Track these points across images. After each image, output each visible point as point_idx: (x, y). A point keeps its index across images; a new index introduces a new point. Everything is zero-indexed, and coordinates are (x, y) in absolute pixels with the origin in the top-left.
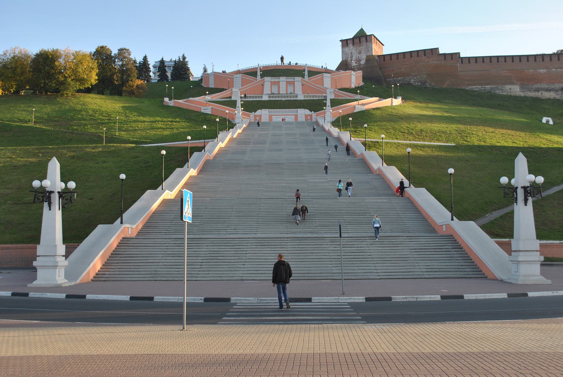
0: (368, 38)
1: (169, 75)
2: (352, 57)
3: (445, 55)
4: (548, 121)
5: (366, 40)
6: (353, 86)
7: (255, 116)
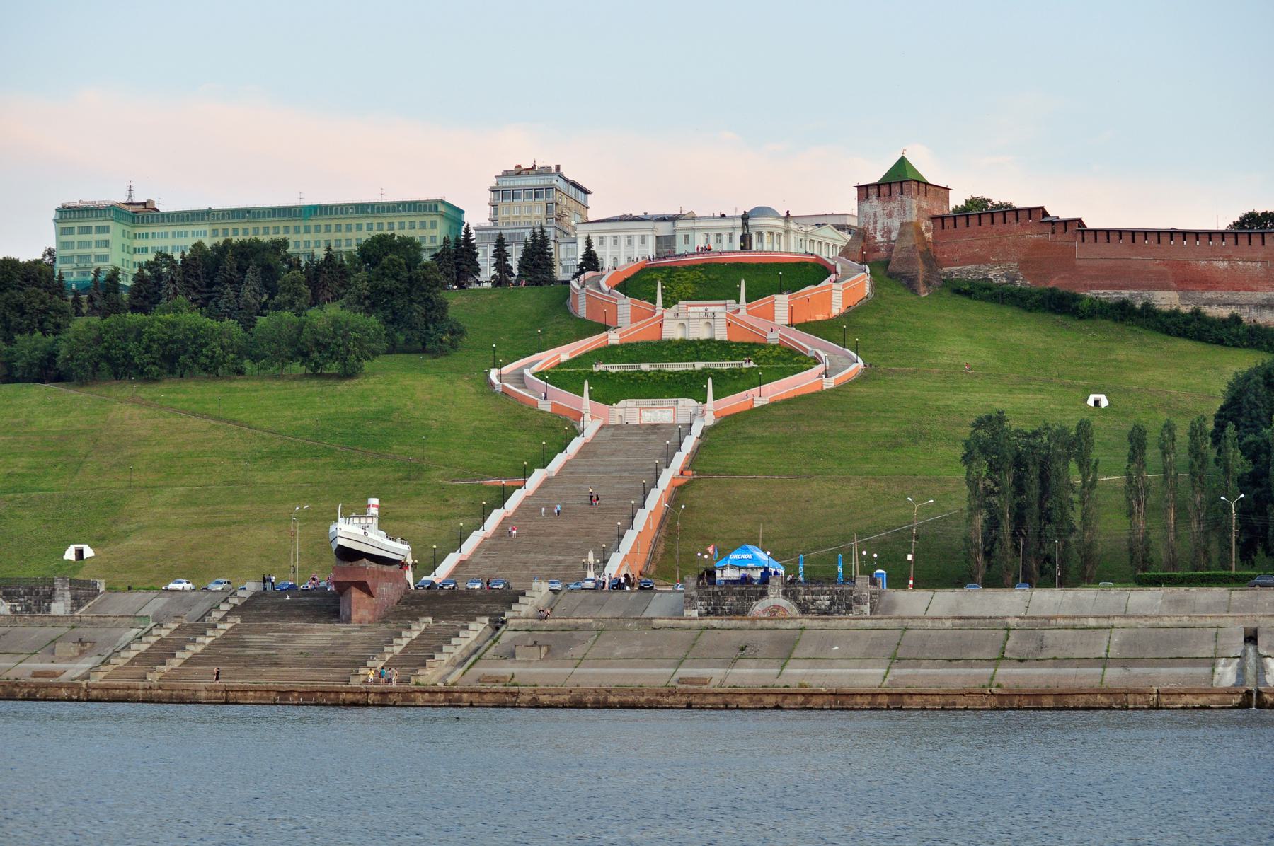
3: (1056, 223)
4: (1097, 403)
6: (836, 311)
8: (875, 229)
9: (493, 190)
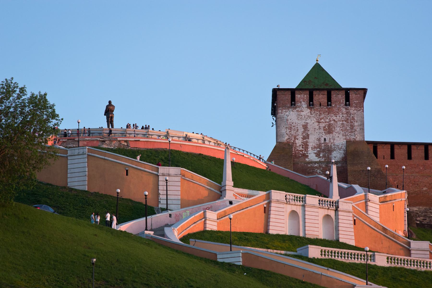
0: (352, 96)
2: (306, 137)
5: (347, 99)
8: (305, 145)
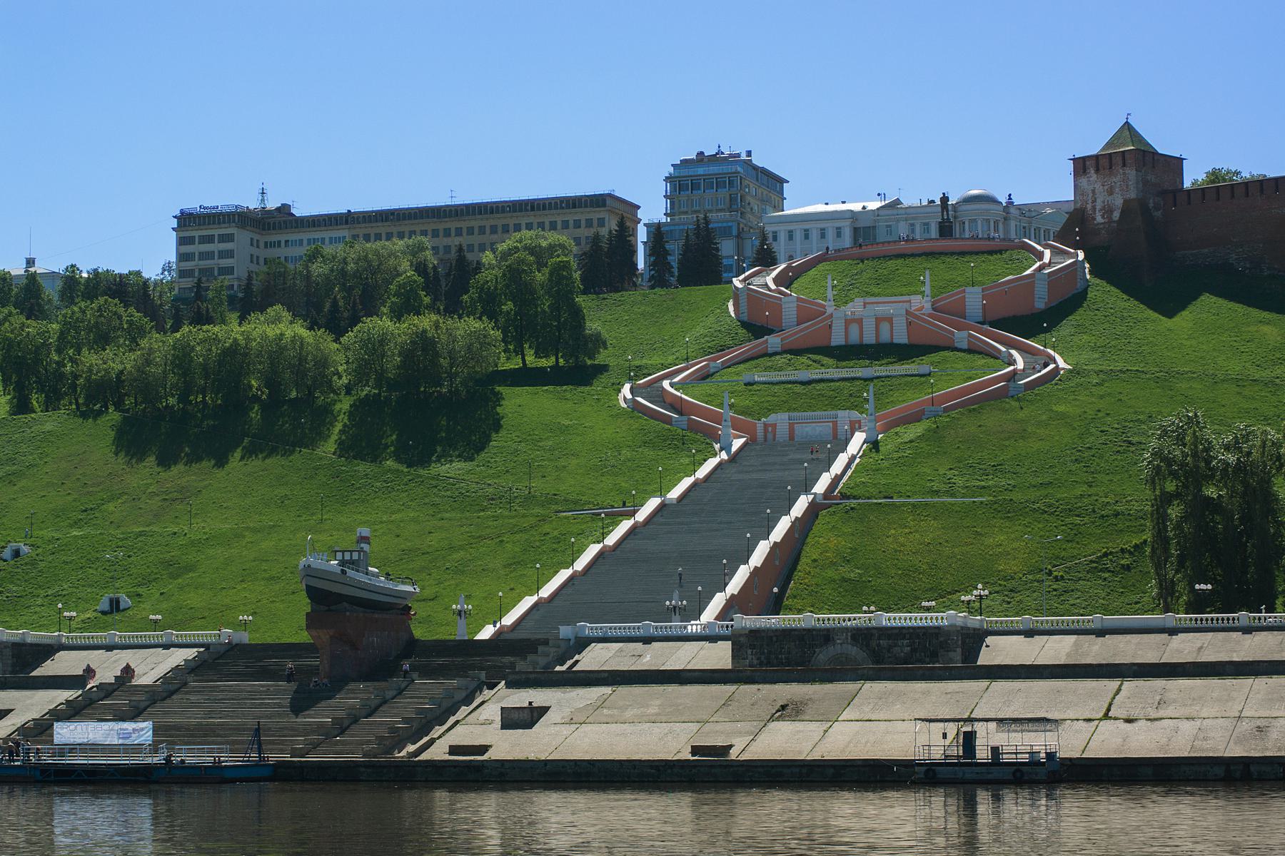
0: (1127, 156)
1: (674, 260)
2: (1094, 201)
6: (1040, 305)
7: (766, 425)
8: (1094, 208)
9: (667, 179)
